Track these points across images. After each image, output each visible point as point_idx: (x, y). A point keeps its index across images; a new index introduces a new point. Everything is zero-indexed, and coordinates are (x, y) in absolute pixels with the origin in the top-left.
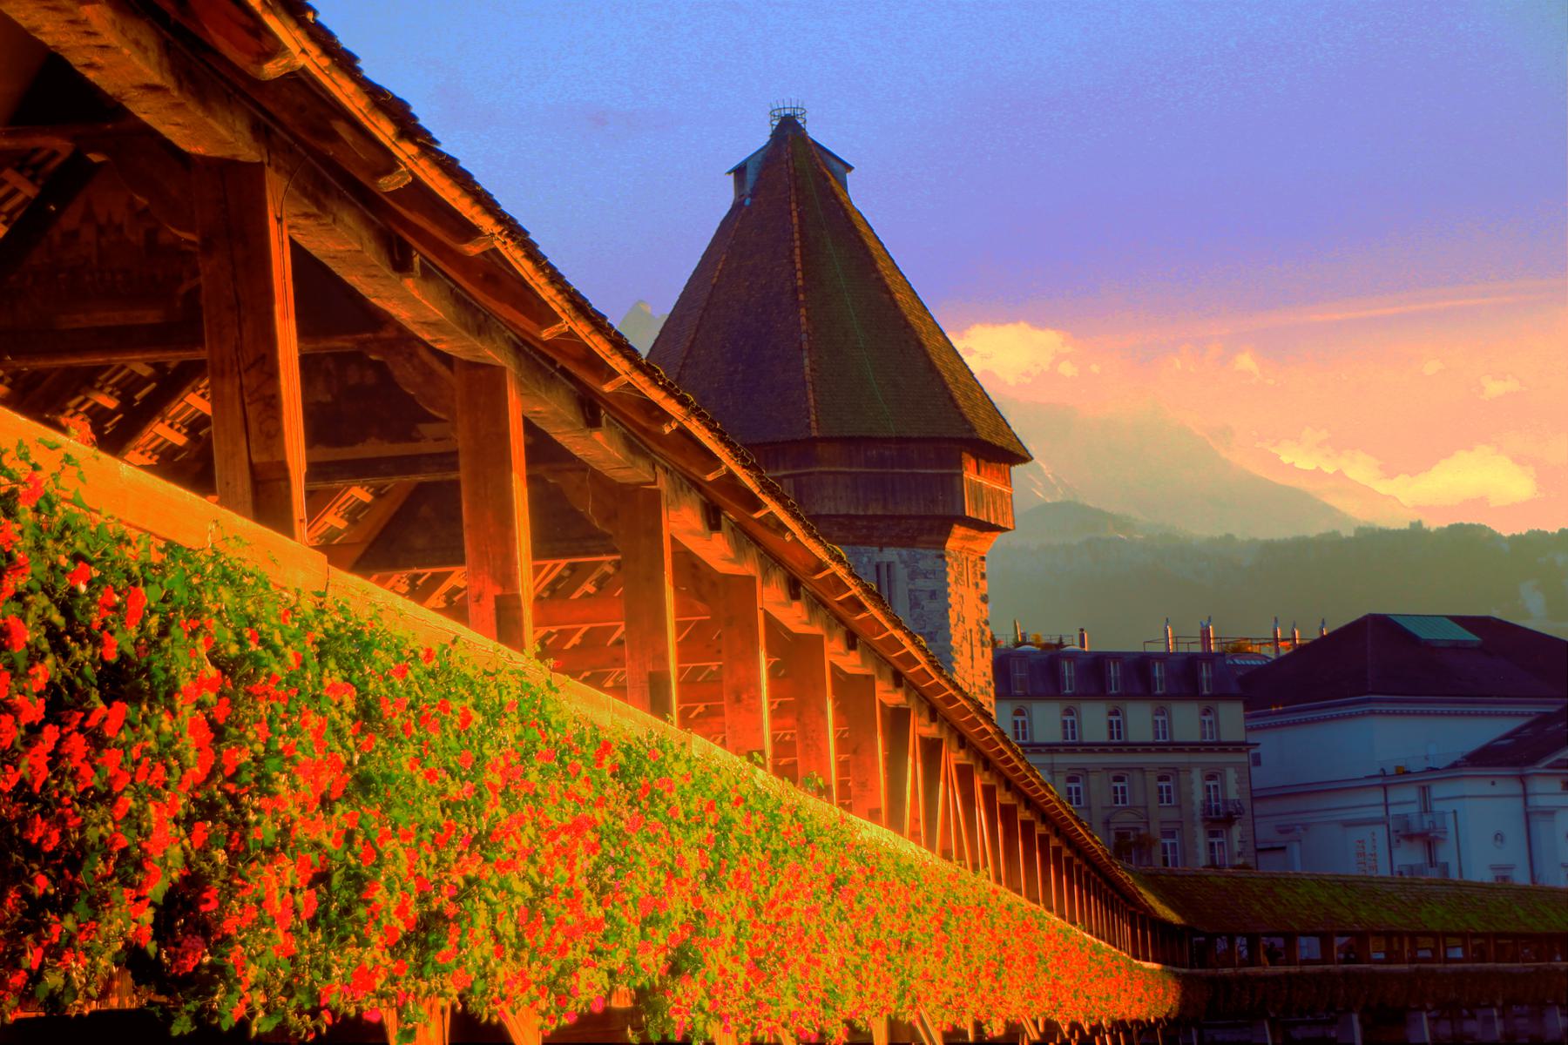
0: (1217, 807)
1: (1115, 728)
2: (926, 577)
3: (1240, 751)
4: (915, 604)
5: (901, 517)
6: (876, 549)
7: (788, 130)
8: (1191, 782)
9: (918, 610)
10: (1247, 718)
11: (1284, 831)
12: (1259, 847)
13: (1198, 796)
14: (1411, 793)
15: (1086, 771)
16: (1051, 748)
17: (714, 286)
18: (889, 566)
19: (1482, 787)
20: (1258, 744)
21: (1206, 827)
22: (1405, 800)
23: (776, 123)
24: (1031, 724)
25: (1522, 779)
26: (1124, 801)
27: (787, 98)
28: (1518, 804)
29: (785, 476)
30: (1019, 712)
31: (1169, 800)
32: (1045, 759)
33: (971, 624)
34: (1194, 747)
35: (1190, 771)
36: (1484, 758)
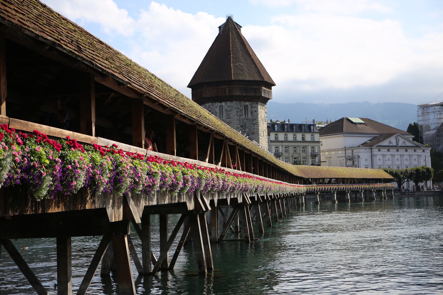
1: (295, 138)
2: (254, 108)
3: (318, 143)
4: (252, 113)
6: (245, 102)
7: (229, 20)
9: (252, 114)
11: (326, 158)
12: (321, 161)
13: (310, 151)
15: (289, 146)
16: (282, 142)
18: (247, 105)
19: (364, 150)
20: (321, 142)
21: (311, 157)
22: (349, 153)
23: (227, 18)
24: (278, 137)
25: (371, 149)
26: (296, 152)
28: (370, 154)
30: (276, 135)
31: (304, 152)
32: (281, 144)
33: (263, 117)
34: (310, 142)
35: (308, 146)
36: (364, 144)
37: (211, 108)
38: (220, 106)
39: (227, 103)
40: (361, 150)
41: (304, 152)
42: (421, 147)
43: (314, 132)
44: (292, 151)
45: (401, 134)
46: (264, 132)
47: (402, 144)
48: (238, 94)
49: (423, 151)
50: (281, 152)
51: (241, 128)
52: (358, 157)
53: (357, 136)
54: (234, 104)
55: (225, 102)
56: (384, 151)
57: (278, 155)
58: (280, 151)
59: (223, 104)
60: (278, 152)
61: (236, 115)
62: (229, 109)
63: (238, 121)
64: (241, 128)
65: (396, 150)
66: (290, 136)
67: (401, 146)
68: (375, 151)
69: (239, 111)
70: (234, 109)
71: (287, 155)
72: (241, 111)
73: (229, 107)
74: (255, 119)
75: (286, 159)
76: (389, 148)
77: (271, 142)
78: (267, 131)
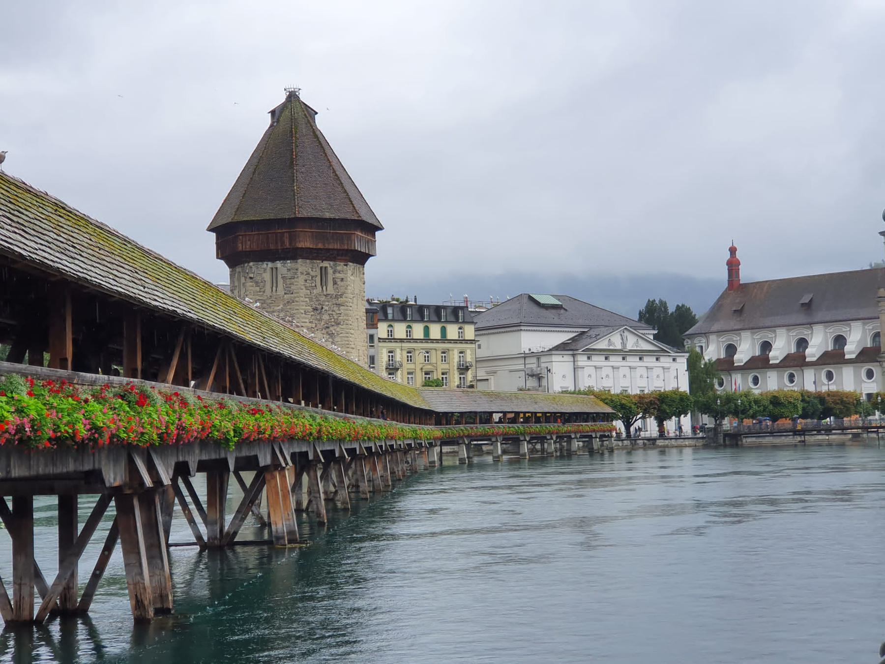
0: (463, 364)
2: (339, 273)
3: (472, 343)
4: (335, 283)
5: (329, 249)
7: (292, 97)
8: (454, 355)
10: (475, 331)
11: (488, 373)
12: (478, 378)
13: (456, 360)
14: (534, 360)
16: (402, 340)
17: (261, 157)
19: (559, 358)
22: (532, 364)
23: (288, 94)
25: (574, 355)
26: (428, 361)
27: (292, 85)
29: (287, 232)
30: (390, 326)
31: (445, 361)
32: (399, 344)
33: (357, 291)
34: (455, 341)
37: (254, 273)
38: (272, 268)
39: (285, 264)
40: (555, 358)
41: (445, 361)
42: (669, 353)
43: (464, 322)
44: (422, 360)
45: (631, 327)
46: (360, 319)
47: (632, 347)
48: (308, 244)
49: (674, 360)
50: (400, 360)
51: (312, 313)
52: (548, 371)
53: (547, 331)
54: (302, 266)
55: (281, 262)
56: (598, 360)
57: (392, 366)
58: (398, 358)
59: (279, 264)
60: (392, 360)
61: (303, 287)
62: (289, 275)
63: (307, 299)
64: (312, 313)
65: (620, 358)
66: (418, 330)
67: (630, 351)
68: (582, 360)
69: (310, 278)
70: (299, 274)
71: (412, 366)
72: (314, 278)
73: (289, 270)
74: (341, 296)
75: (409, 373)
76: (607, 353)
77: (379, 341)
78: (365, 318)
